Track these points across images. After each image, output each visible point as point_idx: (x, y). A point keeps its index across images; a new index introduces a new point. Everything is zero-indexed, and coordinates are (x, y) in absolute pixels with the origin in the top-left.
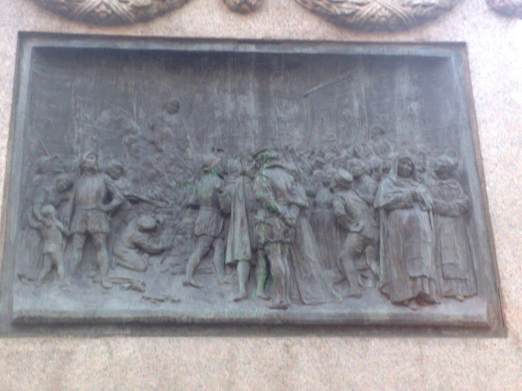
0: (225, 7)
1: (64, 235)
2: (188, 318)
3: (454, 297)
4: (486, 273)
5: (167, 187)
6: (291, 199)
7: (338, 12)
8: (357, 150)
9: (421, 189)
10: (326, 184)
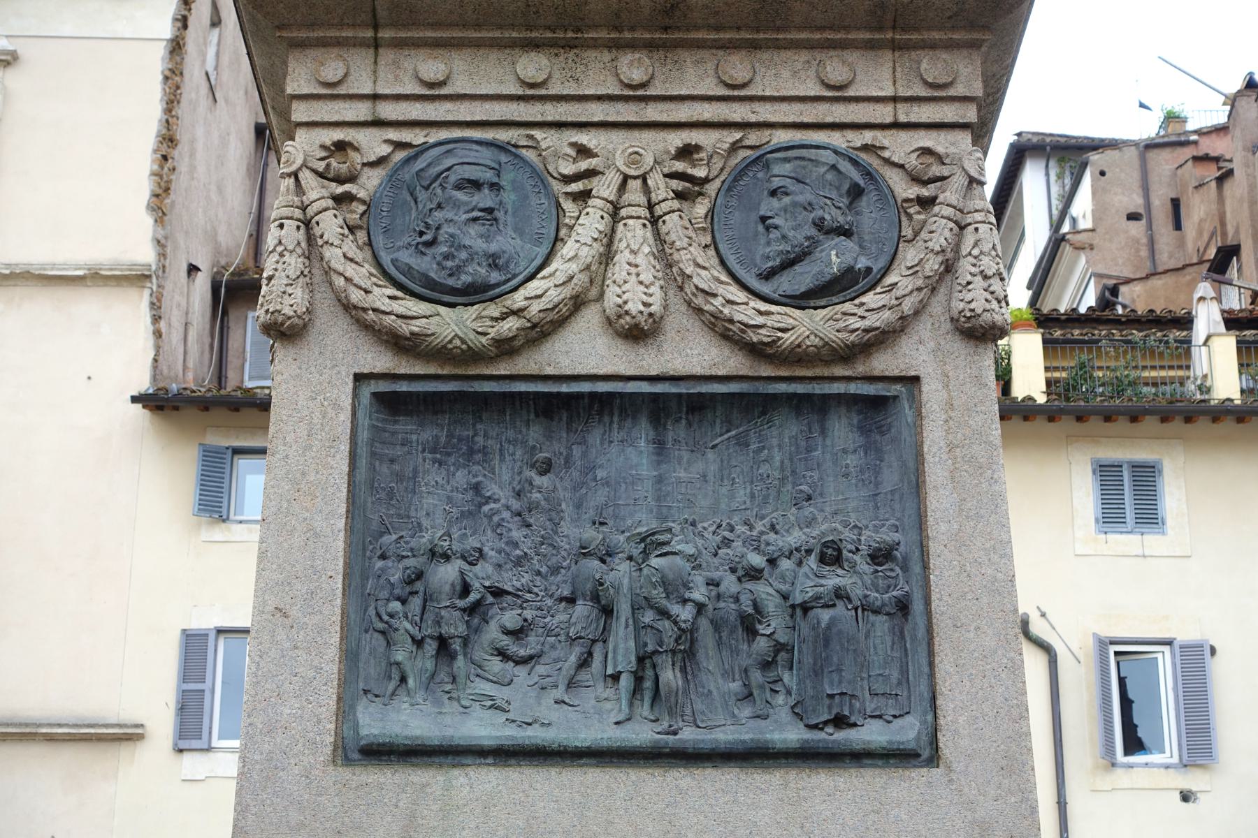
6: (687, 595)
7: (755, 340)
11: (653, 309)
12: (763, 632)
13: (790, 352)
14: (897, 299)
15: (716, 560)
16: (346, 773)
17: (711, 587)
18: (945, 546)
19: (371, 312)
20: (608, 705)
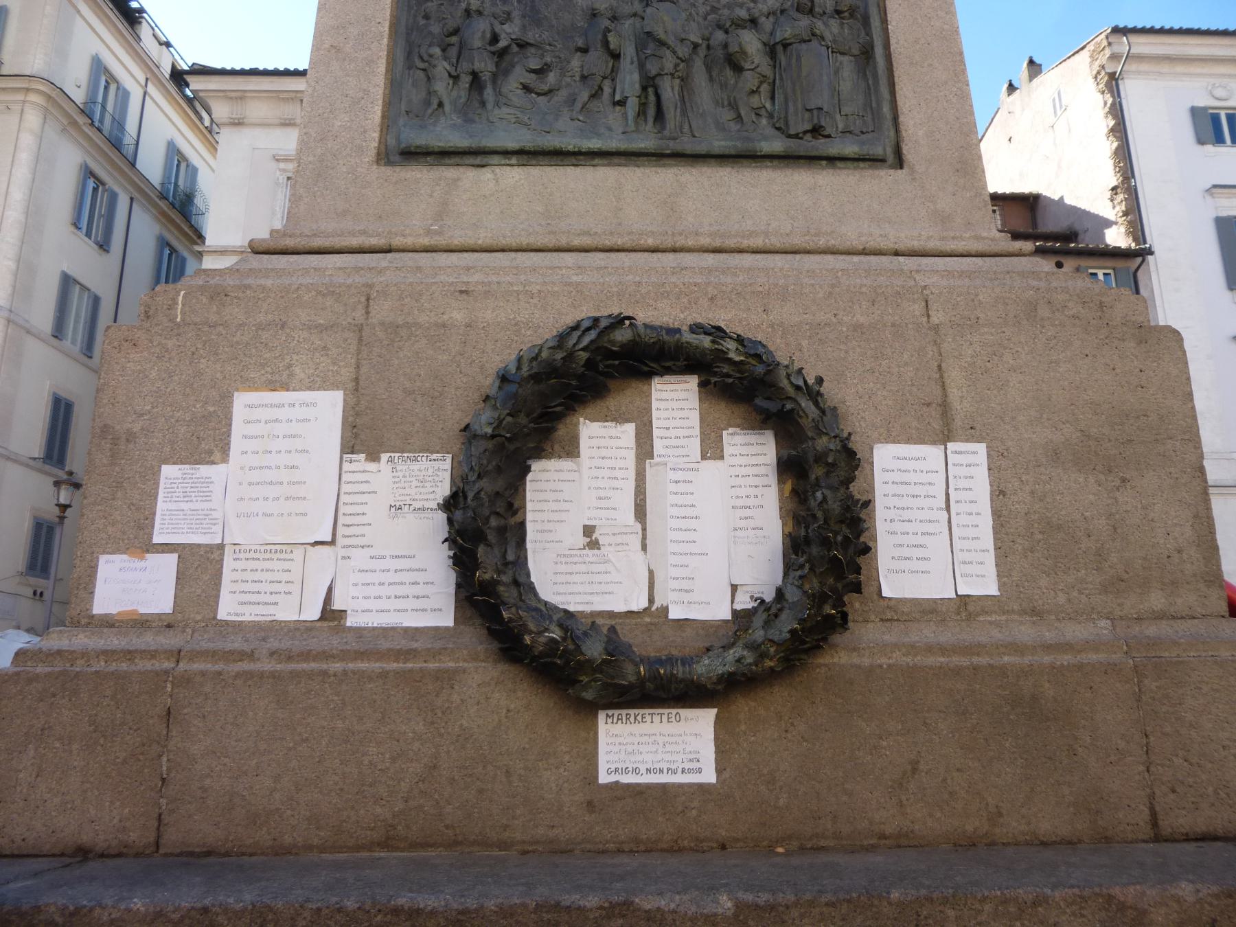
1: (450, 75)
3: (850, 132)
4: (884, 109)
10: (719, 27)
16: (388, 171)
18: (900, 5)
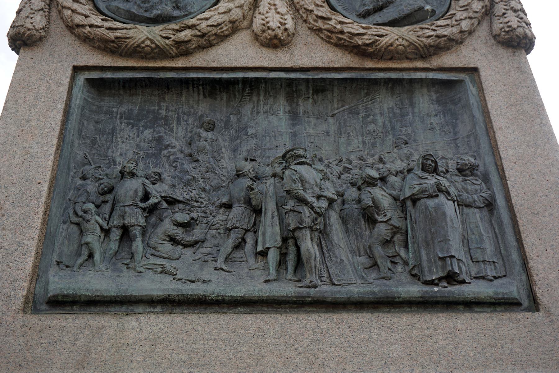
0: (257, 44)
2: (218, 296)
3: (483, 278)
4: (513, 256)
5: (202, 191)
7: (360, 42)
8: (382, 157)
9: (445, 182)
10: (353, 184)
11: (287, 26)
12: (382, 220)
13: (385, 49)
14: (456, 21)
15: (340, 181)
17: (339, 197)
18: (515, 163)
19: (88, 27)
20: (259, 272)
